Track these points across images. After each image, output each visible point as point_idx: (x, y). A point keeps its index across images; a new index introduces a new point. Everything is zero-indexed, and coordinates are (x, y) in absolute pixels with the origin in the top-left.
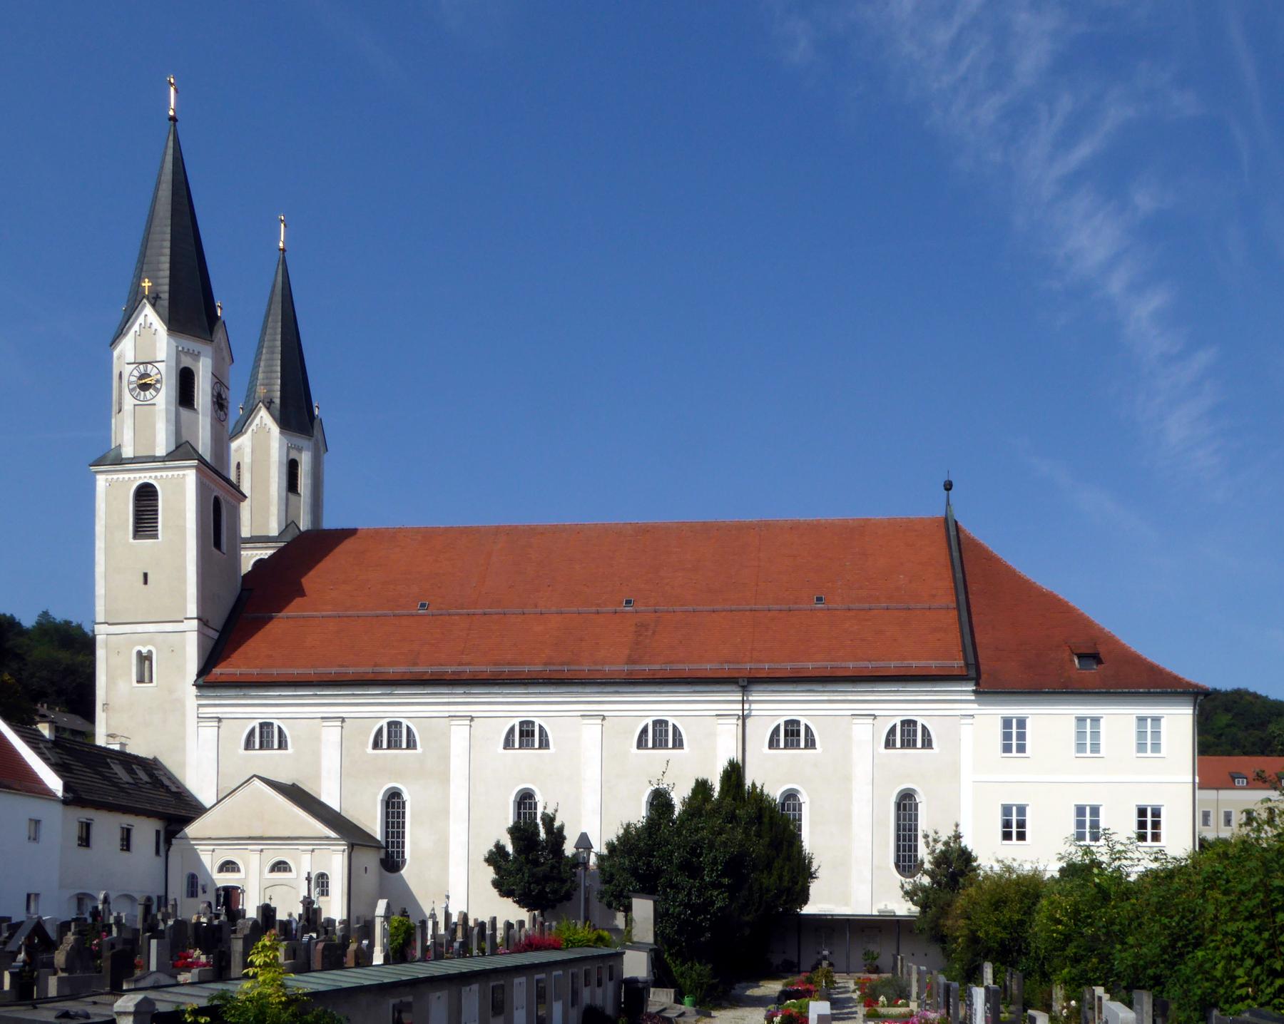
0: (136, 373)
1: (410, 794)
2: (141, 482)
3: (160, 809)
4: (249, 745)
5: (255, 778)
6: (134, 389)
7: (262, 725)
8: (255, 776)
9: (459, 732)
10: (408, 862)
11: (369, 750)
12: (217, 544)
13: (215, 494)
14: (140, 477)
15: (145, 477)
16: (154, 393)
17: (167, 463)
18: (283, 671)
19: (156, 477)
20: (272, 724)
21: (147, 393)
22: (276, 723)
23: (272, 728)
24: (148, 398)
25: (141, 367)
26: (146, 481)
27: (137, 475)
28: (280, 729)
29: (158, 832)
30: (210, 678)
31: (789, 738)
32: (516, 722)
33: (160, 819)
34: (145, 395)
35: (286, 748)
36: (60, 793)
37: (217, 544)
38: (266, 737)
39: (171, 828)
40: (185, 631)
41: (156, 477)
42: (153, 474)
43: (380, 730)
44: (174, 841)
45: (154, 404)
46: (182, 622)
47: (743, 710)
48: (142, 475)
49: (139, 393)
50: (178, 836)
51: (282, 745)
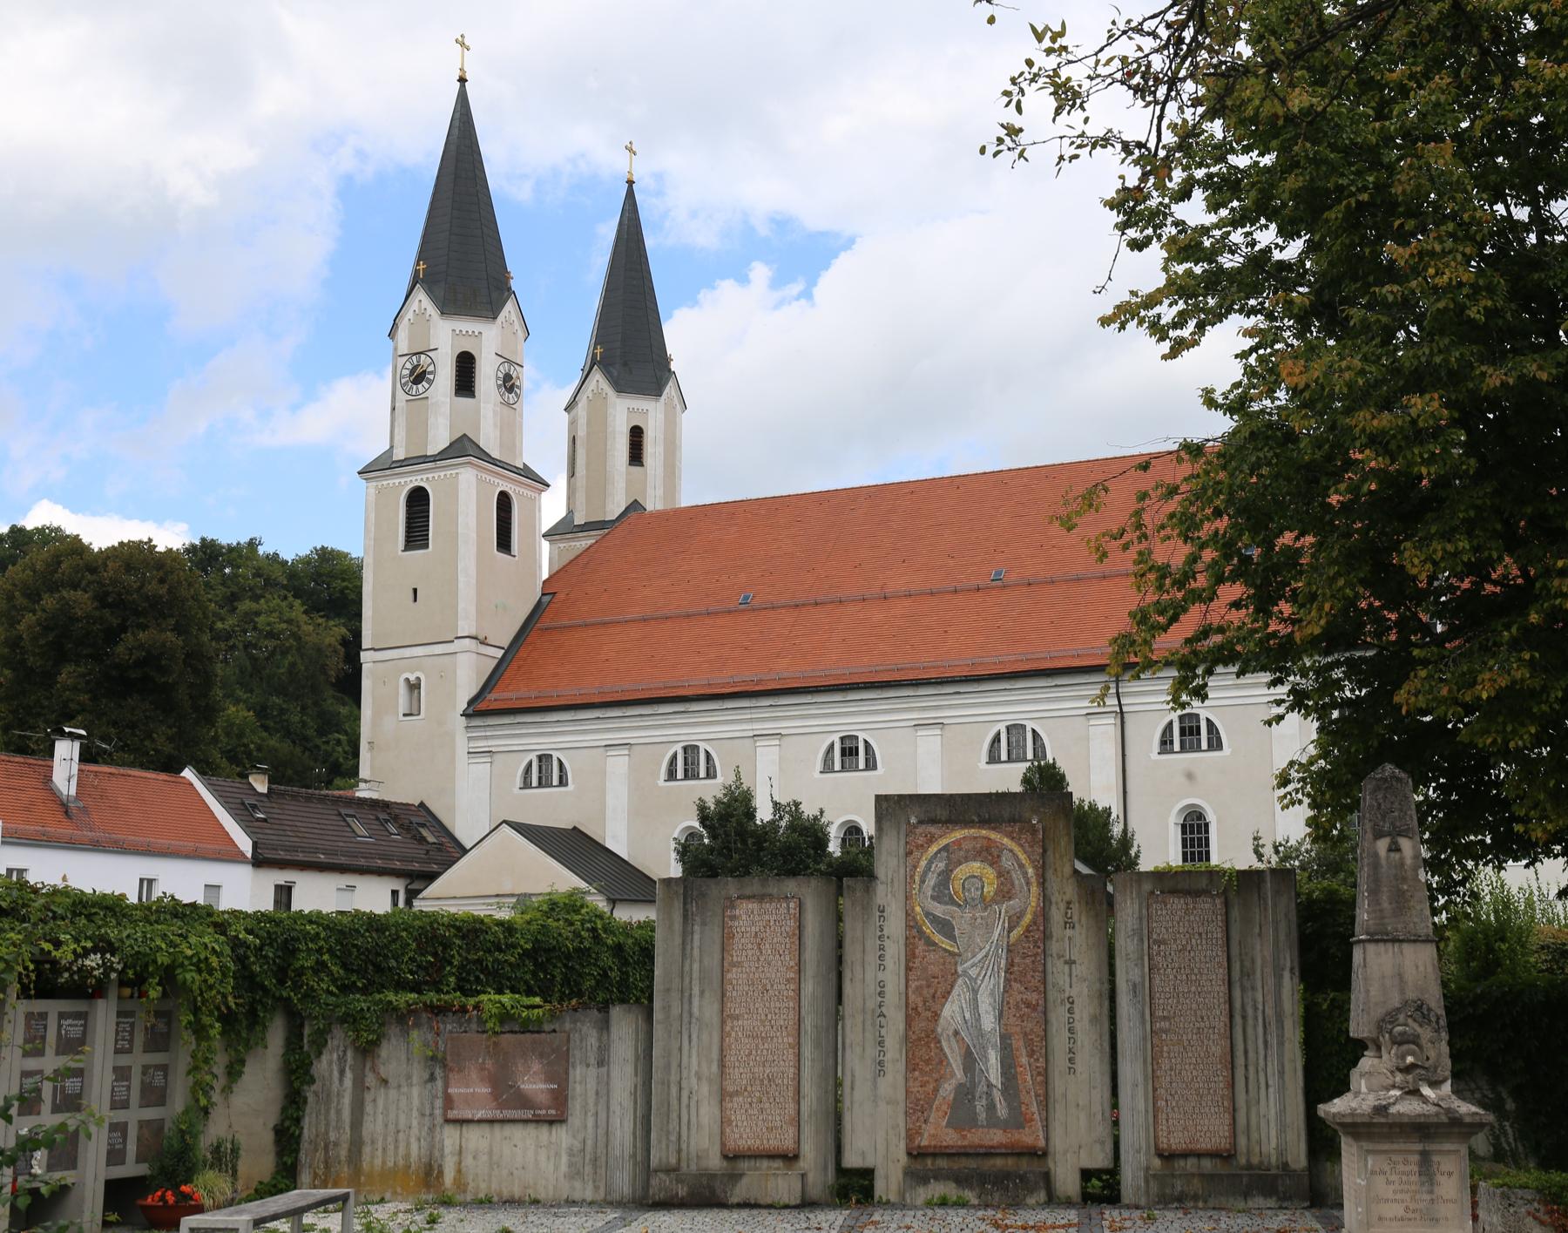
0: (409, 366)
2: (412, 486)
3: (398, 865)
8: (505, 822)
9: (618, 765)
11: (661, 783)
16: (427, 386)
26: (417, 484)
27: (408, 479)
29: (395, 893)
30: (482, 706)
31: (1187, 738)
35: (567, 785)
36: (249, 855)
38: (545, 772)
39: (414, 886)
42: (424, 477)
43: (675, 757)
47: (1120, 705)
48: (414, 478)
49: (411, 388)
50: (420, 896)
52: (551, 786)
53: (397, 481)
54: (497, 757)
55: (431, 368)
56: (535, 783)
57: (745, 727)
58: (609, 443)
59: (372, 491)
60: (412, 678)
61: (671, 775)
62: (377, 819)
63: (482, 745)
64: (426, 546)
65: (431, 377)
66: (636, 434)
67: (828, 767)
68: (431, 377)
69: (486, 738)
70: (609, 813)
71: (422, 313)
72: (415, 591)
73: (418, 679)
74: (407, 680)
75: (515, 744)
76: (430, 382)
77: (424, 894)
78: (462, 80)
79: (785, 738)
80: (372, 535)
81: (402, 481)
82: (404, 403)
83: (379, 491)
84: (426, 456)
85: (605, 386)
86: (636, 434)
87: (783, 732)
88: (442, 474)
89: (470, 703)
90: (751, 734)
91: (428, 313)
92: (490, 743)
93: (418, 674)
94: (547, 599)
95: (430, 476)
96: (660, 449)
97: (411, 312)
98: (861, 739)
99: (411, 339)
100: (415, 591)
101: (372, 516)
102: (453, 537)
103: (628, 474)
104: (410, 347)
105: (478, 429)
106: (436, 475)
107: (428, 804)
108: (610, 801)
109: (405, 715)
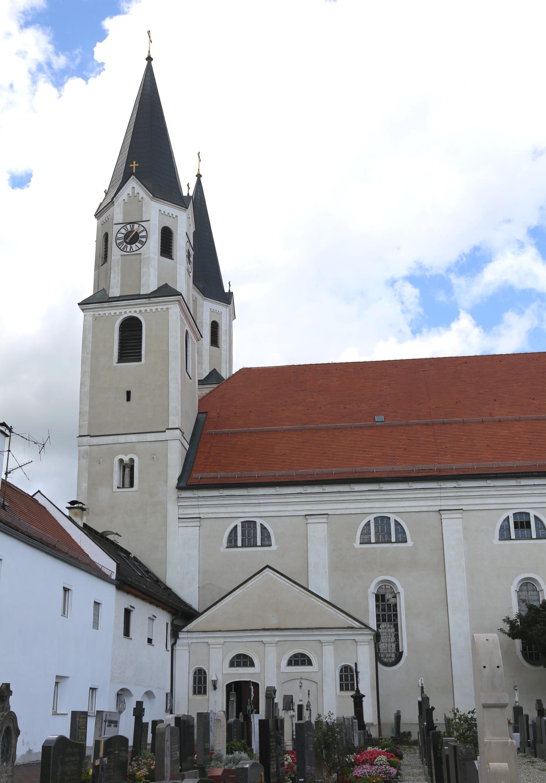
0: (123, 231)
1: (403, 587)
2: (126, 315)
4: (232, 542)
5: (267, 569)
6: (120, 244)
7: (243, 523)
8: (268, 566)
10: (405, 655)
11: (357, 545)
13: (186, 329)
14: (126, 312)
15: (130, 312)
16: (140, 246)
17: (152, 299)
18: (264, 473)
19: (140, 311)
20: (255, 522)
21: (134, 246)
22: (259, 521)
24: (134, 249)
25: (128, 226)
26: (130, 314)
27: (123, 311)
28: (263, 527)
32: (510, 514)
33: (169, 612)
34: (131, 247)
40: (168, 440)
41: (140, 311)
42: (138, 310)
44: (181, 635)
46: (165, 431)
48: (128, 310)
49: (126, 247)
50: (185, 629)
52: (255, 545)
53: (112, 312)
54: (203, 522)
55: (144, 234)
59: (90, 319)
60: (126, 459)
61: (365, 541)
64: (140, 360)
65: (144, 240)
66: (215, 326)
67: (504, 534)
68: (144, 240)
69: (198, 506)
71: (134, 196)
72: (129, 393)
73: (132, 460)
74: (121, 461)
75: (222, 512)
76: (143, 244)
78: (149, 59)
80: (89, 350)
81: (118, 312)
82: (119, 257)
84: (140, 295)
86: (215, 326)
87: (464, 508)
88: (154, 308)
89: (180, 479)
90: (438, 508)
91: (141, 196)
95: (143, 309)
98: (532, 516)
99: (125, 213)
100: (129, 393)
101: (90, 337)
102: (165, 355)
103: (210, 351)
104: (124, 218)
105: (176, 282)
106: (148, 309)
108: (312, 559)
109: (118, 488)
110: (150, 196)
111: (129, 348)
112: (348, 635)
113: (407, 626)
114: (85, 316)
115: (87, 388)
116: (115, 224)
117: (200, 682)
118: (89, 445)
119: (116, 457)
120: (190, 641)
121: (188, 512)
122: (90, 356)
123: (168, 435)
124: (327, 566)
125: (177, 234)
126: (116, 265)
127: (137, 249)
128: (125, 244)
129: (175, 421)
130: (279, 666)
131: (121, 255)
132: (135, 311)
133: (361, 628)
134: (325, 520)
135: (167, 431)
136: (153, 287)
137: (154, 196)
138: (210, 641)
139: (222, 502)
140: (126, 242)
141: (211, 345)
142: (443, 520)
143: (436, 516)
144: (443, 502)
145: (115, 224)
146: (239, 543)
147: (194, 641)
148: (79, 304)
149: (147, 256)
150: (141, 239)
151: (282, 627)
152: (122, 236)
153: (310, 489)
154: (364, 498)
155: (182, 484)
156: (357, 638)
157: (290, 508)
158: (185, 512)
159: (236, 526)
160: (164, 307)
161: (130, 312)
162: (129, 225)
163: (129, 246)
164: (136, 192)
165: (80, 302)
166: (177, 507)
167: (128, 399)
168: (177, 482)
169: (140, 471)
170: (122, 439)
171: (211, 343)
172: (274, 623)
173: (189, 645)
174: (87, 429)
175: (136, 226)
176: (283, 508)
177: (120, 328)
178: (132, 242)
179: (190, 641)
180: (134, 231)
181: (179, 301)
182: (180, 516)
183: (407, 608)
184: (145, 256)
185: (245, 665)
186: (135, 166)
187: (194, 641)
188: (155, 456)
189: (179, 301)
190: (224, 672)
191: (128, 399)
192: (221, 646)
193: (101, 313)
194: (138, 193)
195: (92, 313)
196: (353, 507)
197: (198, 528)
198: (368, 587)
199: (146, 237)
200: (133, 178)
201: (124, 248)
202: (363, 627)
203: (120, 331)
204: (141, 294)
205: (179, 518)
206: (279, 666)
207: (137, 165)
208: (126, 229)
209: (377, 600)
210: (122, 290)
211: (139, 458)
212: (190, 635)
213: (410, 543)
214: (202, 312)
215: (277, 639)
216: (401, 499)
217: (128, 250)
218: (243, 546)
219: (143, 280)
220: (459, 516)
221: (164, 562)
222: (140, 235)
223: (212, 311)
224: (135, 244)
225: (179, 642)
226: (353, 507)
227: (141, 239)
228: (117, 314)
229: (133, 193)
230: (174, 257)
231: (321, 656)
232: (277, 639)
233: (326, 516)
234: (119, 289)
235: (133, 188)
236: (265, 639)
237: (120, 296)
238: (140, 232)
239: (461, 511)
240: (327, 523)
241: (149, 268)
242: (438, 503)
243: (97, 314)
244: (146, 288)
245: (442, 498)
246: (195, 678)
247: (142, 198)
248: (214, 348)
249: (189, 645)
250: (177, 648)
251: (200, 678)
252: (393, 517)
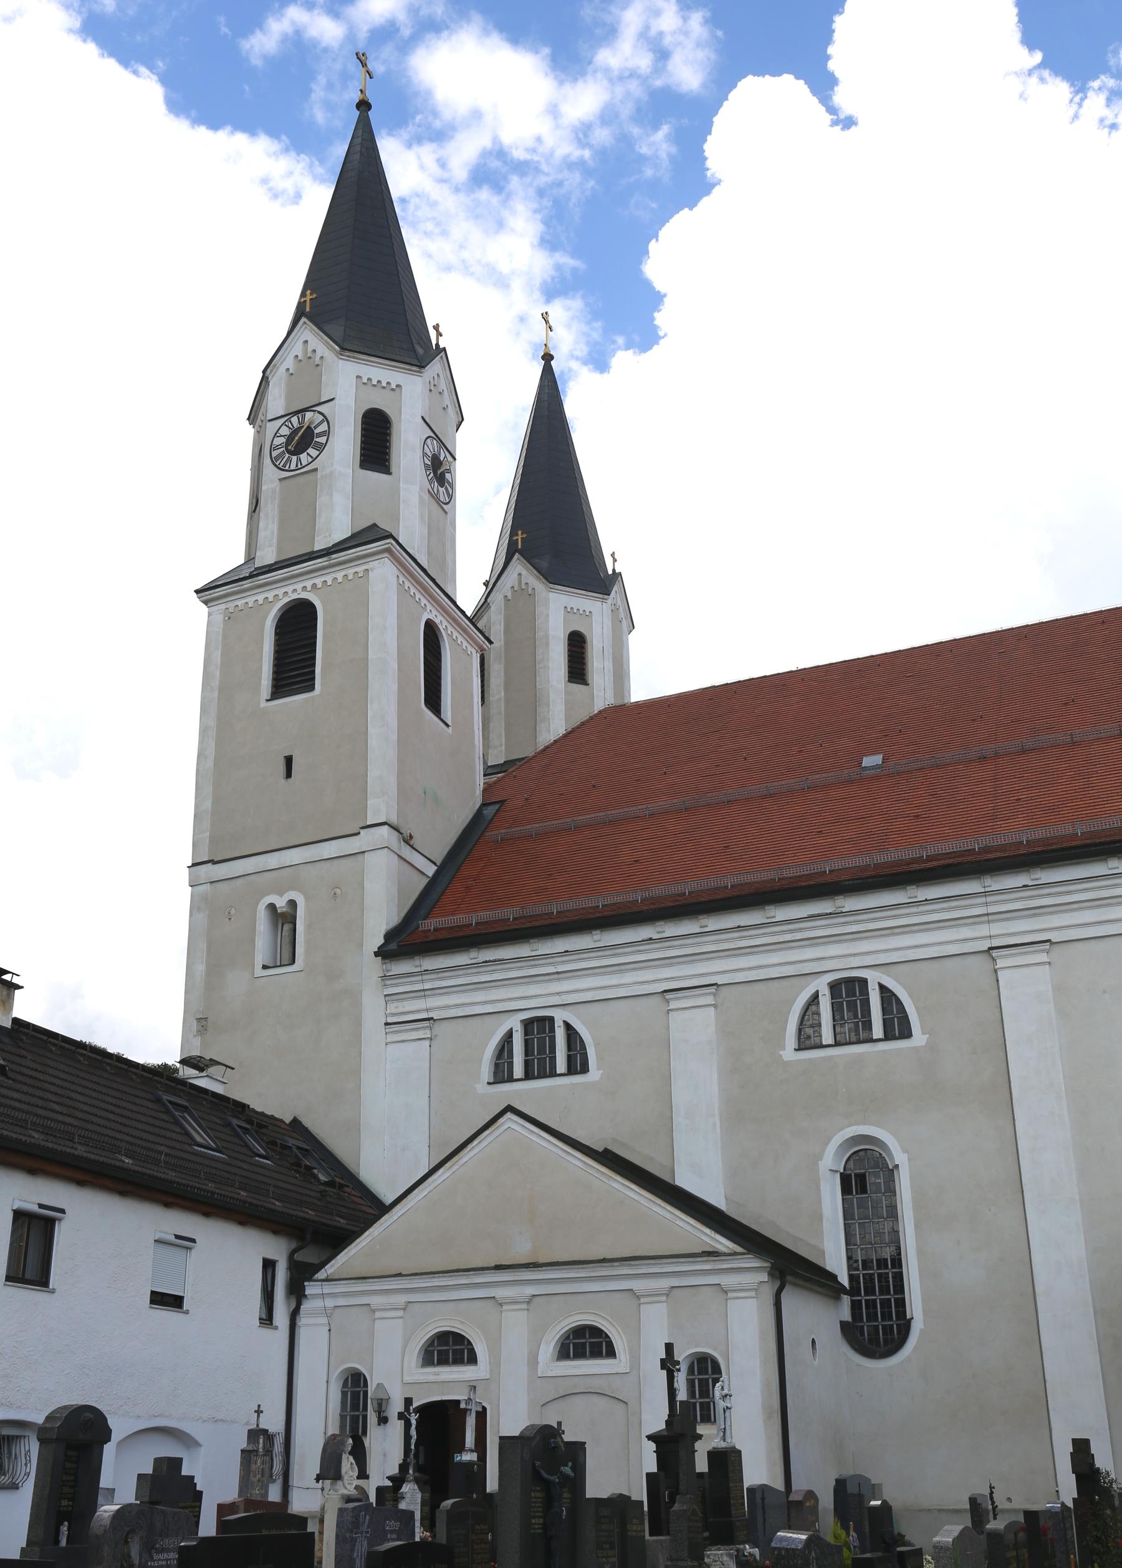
0: (285, 431)
1: (905, 1151)
2: (286, 600)
5: (509, 1115)
6: (277, 458)
7: (528, 1024)
10: (917, 1327)
11: (789, 1052)
12: (433, 700)
17: (334, 556)
18: (571, 905)
19: (314, 586)
21: (303, 456)
22: (560, 1016)
23: (552, 1030)
25: (295, 420)
26: (295, 596)
27: (280, 592)
28: (571, 1032)
29: (269, 1265)
33: (275, 1232)
37: (433, 700)
39: (308, 1256)
40: (364, 852)
41: (314, 586)
42: (309, 584)
44: (311, 1289)
45: (316, 470)
48: (290, 589)
49: (289, 460)
50: (321, 1275)
51: (578, 1064)
52: (553, 1074)
53: (260, 598)
54: (438, 1028)
55: (323, 427)
56: (518, 1070)
57: (965, 932)
58: (539, 651)
59: (219, 618)
60: (281, 903)
61: (807, 1040)
62: (229, 1125)
63: (414, 1007)
64: (312, 688)
65: (323, 440)
66: (577, 644)
68: (323, 440)
69: (423, 993)
70: (679, 1120)
72: (289, 761)
73: (292, 904)
74: (272, 907)
75: (478, 1000)
76: (321, 448)
77: (331, 1269)
79: (1056, 950)
80: (216, 683)
81: (270, 595)
82: (276, 484)
83: (229, 617)
84: (313, 552)
85: (532, 580)
86: (577, 644)
87: (1055, 937)
88: (340, 576)
89: (390, 936)
90: (985, 944)
91: (319, 354)
92: (432, 1002)
93: (292, 895)
94: (490, 811)
95: (318, 581)
96: (609, 665)
97: (291, 358)
99: (290, 396)
100: (289, 761)
102: (361, 668)
105: (396, 518)
107: (307, 1122)
108: (681, 1095)
109: (265, 967)
110: (335, 350)
111: (292, 667)
112: (702, 1274)
113: (920, 1252)
114: (210, 614)
115: (210, 763)
116: (270, 420)
117: (355, 1407)
118: (211, 882)
119: (262, 902)
120: (330, 1303)
121: (407, 1009)
122: (216, 694)
123: (366, 839)
124: (717, 1111)
125: (400, 421)
126: (270, 501)
127: (310, 460)
128: (287, 455)
129: (380, 807)
130: (533, 1361)
131: (280, 480)
132: (304, 588)
133: (735, 1254)
134: (710, 1000)
135: (363, 832)
136: (342, 532)
137: (342, 348)
138: (375, 1301)
139: (475, 979)
140: (289, 452)
141: (570, 681)
142: (999, 973)
143: (980, 964)
144: (996, 928)
145: (270, 420)
146: (518, 1070)
147: (341, 1302)
148: (197, 592)
149: (328, 471)
150: (317, 440)
151: (542, 1260)
152: (283, 440)
153: (671, 929)
154: (799, 936)
155: (393, 946)
156: (726, 1280)
157: (628, 978)
158: (401, 1010)
159: (509, 1035)
160: (360, 569)
161: (295, 590)
162: (296, 417)
163: (294, 458)
164: (310, 349)
165: (198, 587)
166: (382, 1001)
167: (289, 774)
168: (382, 941)
169: (309, 927)
170: (273, 861)
171: (569, 677)
172: (522, 1251)
173: (328, 1313)
174: (207, 849)
175: (309, 415)
176: (613, 980)
177: (277, 627)
178: (298, 450)
179: (330, 1303)
180: (303, 426)
181: (388, 550)
182: (390, 1020)
183: (917, 1205)
184: (324, 473)
185: (458, 1361)
186: (310, 299)
187: (341, 1302)
188: (338, 891)
189: (388, 550)
190: (407, 1379)
191: (289, 774)
192: (400, 1313)
193: (240, 603)
194: (314, 351)
195: (223, 607)
196: (773, 963)
197: (427, 1043)
198: (819, 1156)
199: (327, 433)
200: (305, 323)
201: (284, 466)
202: (723, 1244)
203: (276, 634)
204: (316, 549)
205: (387, 1024)
206: (533, 1361)
207: (314, 296)
208: (290, 426)
209: (846, 1189)
210: (280, 549)
211: (307, 899)
212: (328, 1288)
213: (919, 1037)
214: (547, 616)
215: (530, 1290)
216: (891, 931)
217: (293, 467)
218: (528, 1075)
219: (320, 522)
220: (1043, 957)
221: (354, 1127)
222: (316, 431)
223: (569, 611)
224: (306, 453)
225: (306, 1306)
226: (773, 963)
227: (317, 440)
228: (270, 600)
229: (305, 351)
230: (393, 469)
231: (635, 1331)
232: (530, 1290)
233: (712, 989)
234: (274, 549)
235: (306, 342)
236: (500, 1293)
237: (276, 563)
238: (316, 427)
239: (1047, 946)
240: (715, 1006)
241: (331, 496)
242: (983, 930)
243: (231, 605)
244: (325, 537)
245: (991, 917)
246: (344, 1394)
247: (322, 357)
248: (577, 688)
249: (328, 1313)
250: (303, 1321)
251: (355, 1396)
252: (874, 979)
